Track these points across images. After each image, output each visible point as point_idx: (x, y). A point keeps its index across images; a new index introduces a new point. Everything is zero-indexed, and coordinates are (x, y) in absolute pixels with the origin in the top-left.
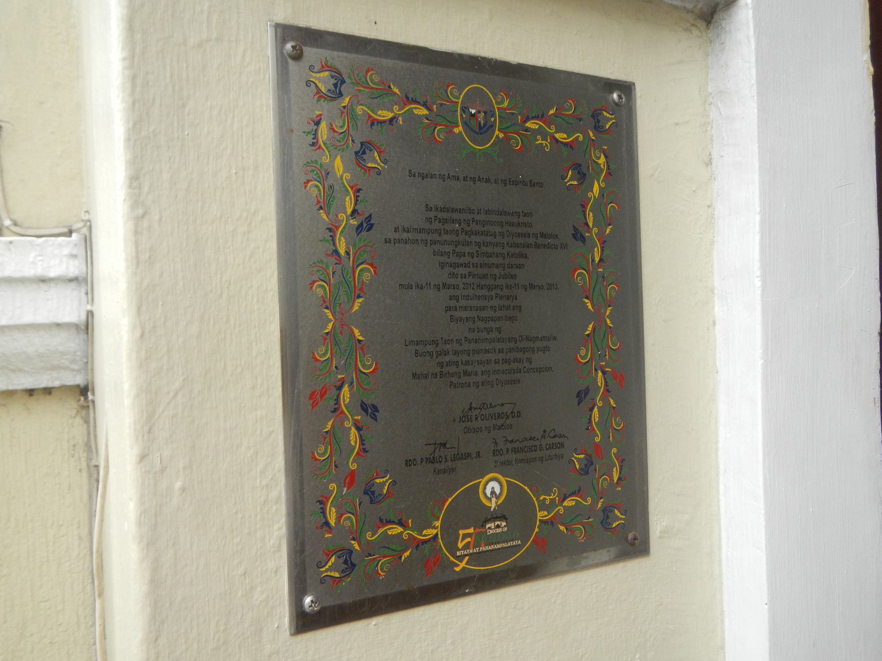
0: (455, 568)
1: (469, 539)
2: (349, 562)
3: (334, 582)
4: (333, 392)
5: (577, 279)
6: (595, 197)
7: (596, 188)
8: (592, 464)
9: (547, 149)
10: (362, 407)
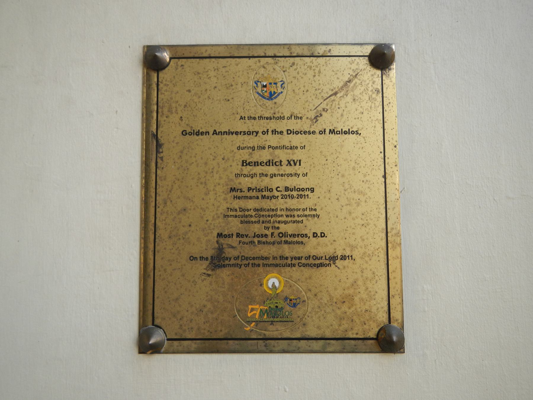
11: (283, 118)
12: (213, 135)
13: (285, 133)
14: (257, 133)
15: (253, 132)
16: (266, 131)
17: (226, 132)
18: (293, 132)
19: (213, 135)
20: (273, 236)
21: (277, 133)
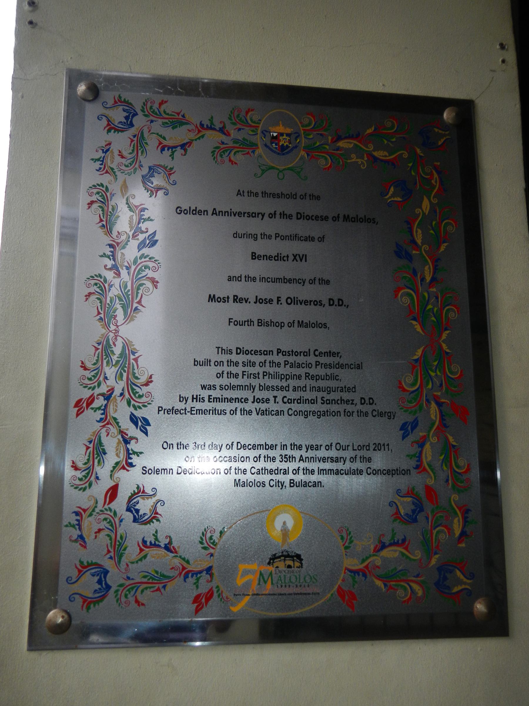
0: (232, 608)
1: (250, 577)
2: (104, 582)
3: (84, 602)
4: (100, 402)
5: (401, 300)
6: (424, 214)
7: (426, 204)
8: (422, 510)
9: (364, 166)
10: (131, 419)
11: (295, 197)
12: (212, 215)
13: (295, 216)
14: (263, 216)
15: (258, 214)
16: (273, 213)
17: (228, 212)
18: (304, 216)
19: (212, 215)
20: (280, 302)
21: (285, 216)
